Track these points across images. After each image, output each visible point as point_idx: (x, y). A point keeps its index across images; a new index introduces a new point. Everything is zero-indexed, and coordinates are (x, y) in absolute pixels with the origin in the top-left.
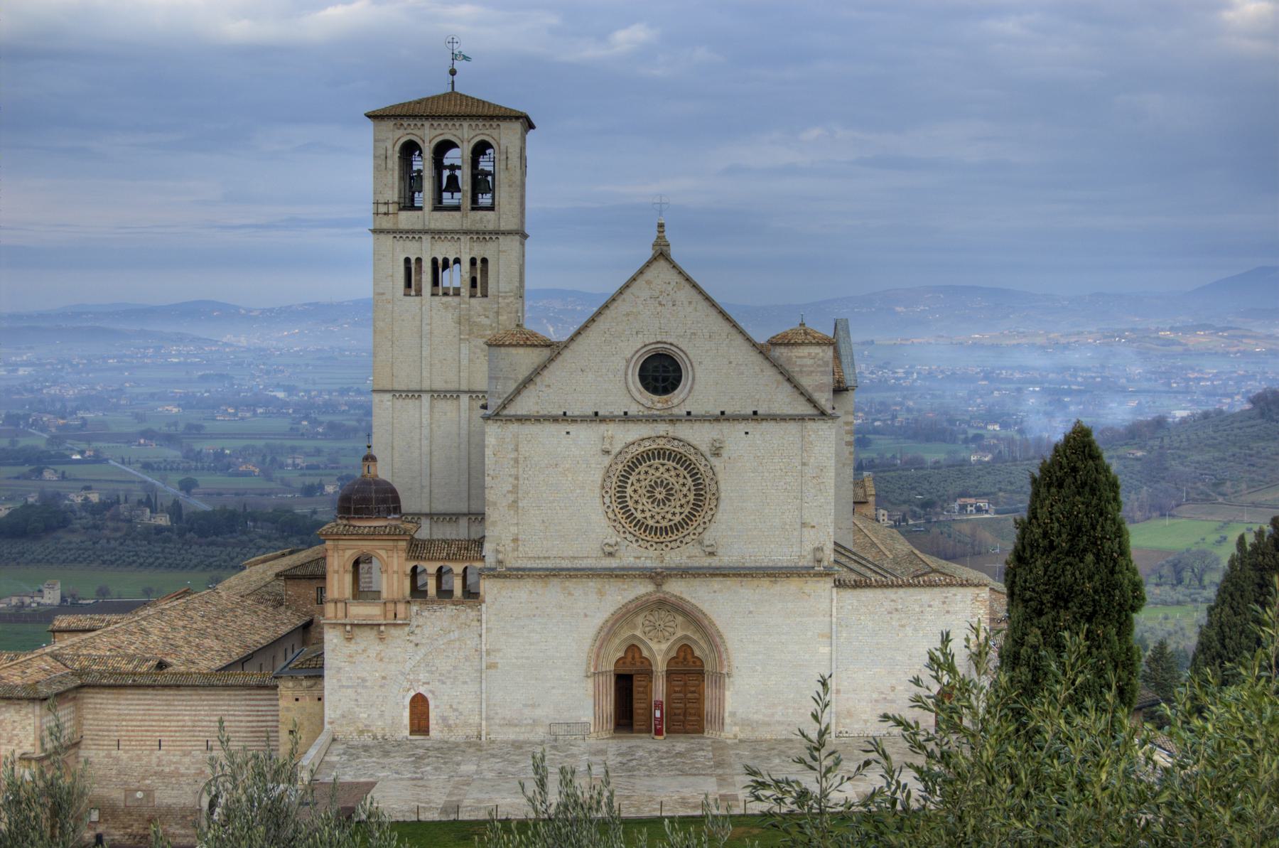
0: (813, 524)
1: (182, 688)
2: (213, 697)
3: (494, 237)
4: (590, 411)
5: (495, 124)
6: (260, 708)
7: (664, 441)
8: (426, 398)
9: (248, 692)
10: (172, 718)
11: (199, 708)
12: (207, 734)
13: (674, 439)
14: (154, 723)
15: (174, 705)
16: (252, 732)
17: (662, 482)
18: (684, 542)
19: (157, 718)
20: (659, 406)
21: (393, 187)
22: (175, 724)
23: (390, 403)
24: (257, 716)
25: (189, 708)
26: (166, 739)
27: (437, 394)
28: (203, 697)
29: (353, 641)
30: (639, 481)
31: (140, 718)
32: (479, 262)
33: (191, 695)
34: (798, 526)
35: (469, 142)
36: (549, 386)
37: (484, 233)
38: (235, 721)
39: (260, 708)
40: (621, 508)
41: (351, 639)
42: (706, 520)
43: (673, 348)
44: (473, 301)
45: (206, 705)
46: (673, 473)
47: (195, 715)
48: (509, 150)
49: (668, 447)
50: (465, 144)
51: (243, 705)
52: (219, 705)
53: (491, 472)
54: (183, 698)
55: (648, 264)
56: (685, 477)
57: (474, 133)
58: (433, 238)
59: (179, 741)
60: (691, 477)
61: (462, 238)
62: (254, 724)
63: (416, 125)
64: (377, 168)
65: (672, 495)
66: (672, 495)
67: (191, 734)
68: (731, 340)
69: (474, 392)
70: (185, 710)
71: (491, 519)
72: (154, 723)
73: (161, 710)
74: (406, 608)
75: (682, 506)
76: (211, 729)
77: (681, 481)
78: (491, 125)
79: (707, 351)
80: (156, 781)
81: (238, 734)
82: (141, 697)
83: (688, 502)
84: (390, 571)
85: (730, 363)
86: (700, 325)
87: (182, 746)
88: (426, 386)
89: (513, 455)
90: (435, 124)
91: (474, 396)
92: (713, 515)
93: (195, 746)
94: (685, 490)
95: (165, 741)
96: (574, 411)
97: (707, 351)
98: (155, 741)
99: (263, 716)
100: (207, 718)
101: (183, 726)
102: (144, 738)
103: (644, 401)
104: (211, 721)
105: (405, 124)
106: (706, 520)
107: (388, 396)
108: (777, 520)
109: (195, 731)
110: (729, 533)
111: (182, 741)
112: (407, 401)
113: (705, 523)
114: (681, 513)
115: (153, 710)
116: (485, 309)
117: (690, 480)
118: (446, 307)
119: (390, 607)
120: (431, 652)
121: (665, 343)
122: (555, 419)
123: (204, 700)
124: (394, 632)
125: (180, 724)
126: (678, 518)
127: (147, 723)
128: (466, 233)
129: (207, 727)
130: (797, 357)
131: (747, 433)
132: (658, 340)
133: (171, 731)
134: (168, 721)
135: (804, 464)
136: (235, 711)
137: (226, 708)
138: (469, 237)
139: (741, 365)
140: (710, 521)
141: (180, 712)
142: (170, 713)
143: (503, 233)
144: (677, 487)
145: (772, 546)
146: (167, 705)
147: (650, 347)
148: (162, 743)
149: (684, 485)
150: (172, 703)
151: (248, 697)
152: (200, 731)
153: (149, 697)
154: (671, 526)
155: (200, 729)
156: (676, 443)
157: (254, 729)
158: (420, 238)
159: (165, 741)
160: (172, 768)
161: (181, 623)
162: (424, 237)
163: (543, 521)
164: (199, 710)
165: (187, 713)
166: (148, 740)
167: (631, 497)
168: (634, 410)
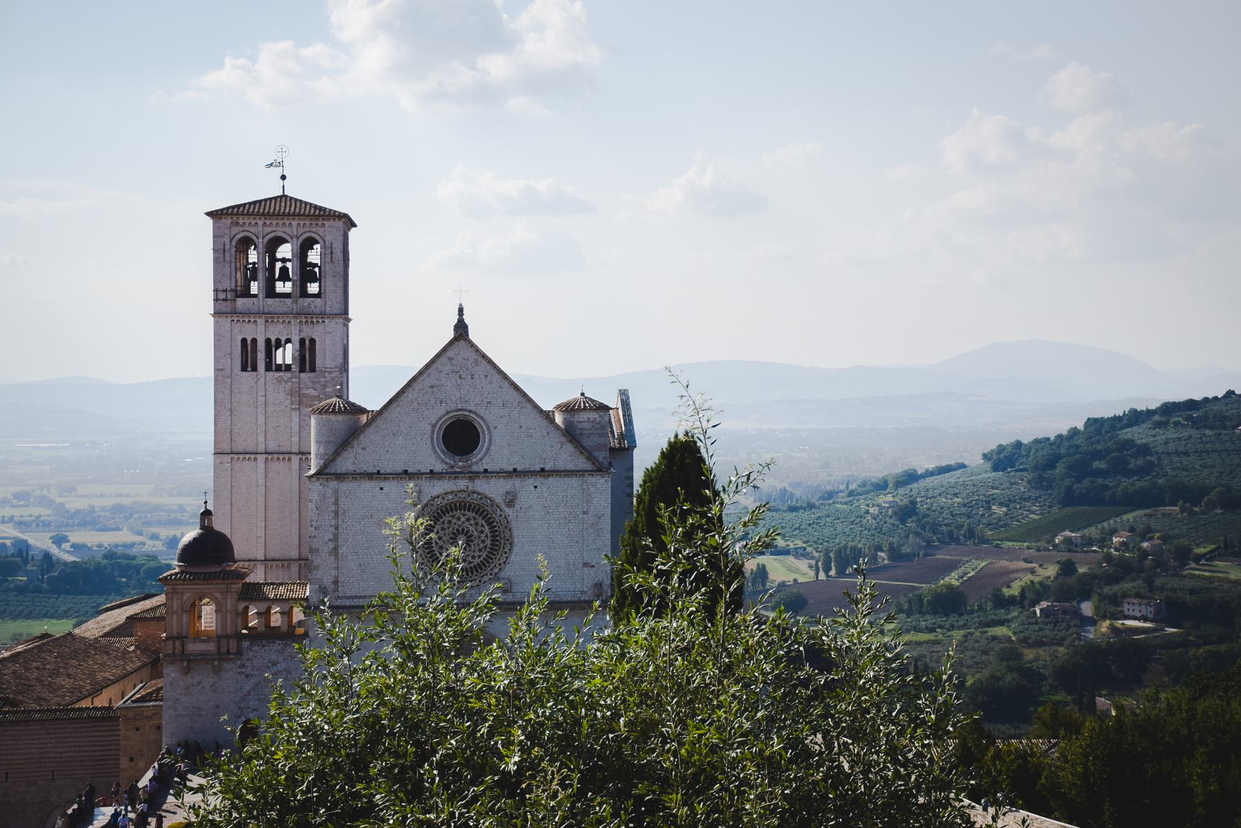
0: (593, 564)
2: (60, 731)
4: (400, 469)
5: (320, 223)
6: (104, 739)
7: (465, 494)
9: (93, 724)
10: (19, 751)
11: (46, 741)
12: (53, 765)
13: (473, 493)
16: (96, 760)
17: (463, 529)
18: (483, 581)
20: (461, 464)
21: (231, 278)
23: (229, 465)
25: (35, 742)
29: (190, 674)
30: (443, 529)
32: (307, 342)
34: (580, 566)
35: (298, 238)
36: (364, 449)
39: (104, 739)
40: (428, 553)
41: (187, 673)
42: (501, 562)
43: (471, 415)
44: (303, 375)
45: (52, 738)
46: (472, 522)
47: (42, 748)
48: (334, 246)
49: (468, 499)
50: (295, 240)
53: (314, 523)
55: (451, 343)
56: (483, 526)
57: (301, 230)
58: (267, 321)
60: (488, 525)
61: (293, 321)
63: (250, 223)
64: (216, 261)
65: (472, 541)
66: (472, 541)
68: (522, 408)
70: (33, 744)
71: (314, 564)
74: (238, 644)
75: (480, 550)
77: (480, 528)
78: (317, 224)
79: (501, 417)
83: (485, 547)
84: (224, 610)
85: (521, 427)
86: (495, 395)
88: (261, 448)
89: (333, 508)
90: (268, 222)
91: (304, 458)
92: (507, 558)
94: (483, 536)
96: (387, 468)
97: (501, 417)
99: (106, 745)
100: (53, 750)
101: (30, 759)
103: (449, 461)
104: (57, 753)
105: (241, 222)
106: (501, 562)
107: (227, 458)
108: (562, 561)
110: (522, 573)
113: (500, 564)
114: (480, 557)
116: (314, 383)
117: (487, 528)
118: (279, 380)
119: (223, 642)
120: (260, 682)
121: (465, 410)
122: (370, 476)
124: (227, 665)
126: (477, 561)
130: (578, 422)
131: (536, 487)
132: (459, 408)
135: (584, 513)
139: (531, 429)
140: (504, 563)
144: (476, 533)
145: (558, 583)
147: (452, 414)
148: (9, 776)
149: (482, 532)
151: (93, 729)
152: (46, 762)
154: (471, 568)
156: (475, 495)
157: (98, 758)
158: (255, 321)
161: (35, 664)
162: (258, 320)
163: (360, 565)
165: (35, 746)
167: (437, 543)
168: (438, 467)
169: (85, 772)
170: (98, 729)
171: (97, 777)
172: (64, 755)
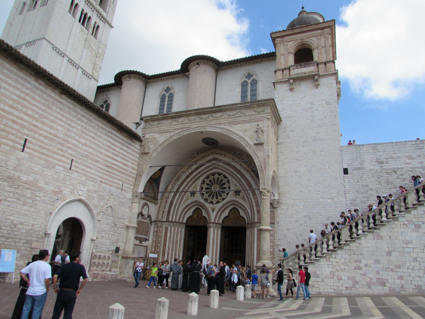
1: (63, 96)
2: (86, 121)
3: (104, 21)
6: (116, 148)
8: (66, 59)
9: (111, 130)
10: (46, 121)
11: (72, 124)
12: (74, 153)
14: (25, 117)
15: (52, 109)
19: (30, 113)
22: (48, 129)
24: (113, 153)
26: (33, 140)
27: (71, 62)
28: (79, 116)
31: (11, 102)
33: (69, 108)
37: (102, 17)
38: (97, 151)
39: (116, 148)
44: (92, 36)
45: (79, 125)
51: (105, 139)
52: (89, 130)
54: (62, 107)
59: (46, 149)
61: (95, 11)
62: (110, 160)
67: (59, 146)
69: (84, 70)
70: (60, 120)
72: (25, 117)
73: (38, 107)
76: (78, 149)
80: (8, 189)
81: (97, 164)
82: (20, 80)
87: (48, 156)
93: (60, 161)
95: (32, 143)
98: (21, 138)
99: (116, 155)
100: (77, 138)
102: (9, 130)
104: (79, 142)
107: (52, 46)
109: (62, 145)
111: (49, 150)
112: (57, 54)
115: (28, 102)
123: (79, 119)
125: (53, 131)
127: (17, 113)
128: (97, 11)
129: (75, 145)
133: (41, 135)
134: (42, 123)
136: (100, 142)
137: (93, 135)
138: (97, 13)
141: (56, 120)
142: (46, 114)
143: (108, 23)
146: (44, 104)
150: (50, 106)
151: (110, 134)
152: (68, 148)
153: (28, 85)
155: (69, 145)
157: (108, 164)
159: (32, 143)
160: (31, 178)
164: (73, 127)
165: (62, 123)
166: (12, 134)
169: (97, 173)
170: (113, 136)
171: (105, 183)
172: (84, 147)
